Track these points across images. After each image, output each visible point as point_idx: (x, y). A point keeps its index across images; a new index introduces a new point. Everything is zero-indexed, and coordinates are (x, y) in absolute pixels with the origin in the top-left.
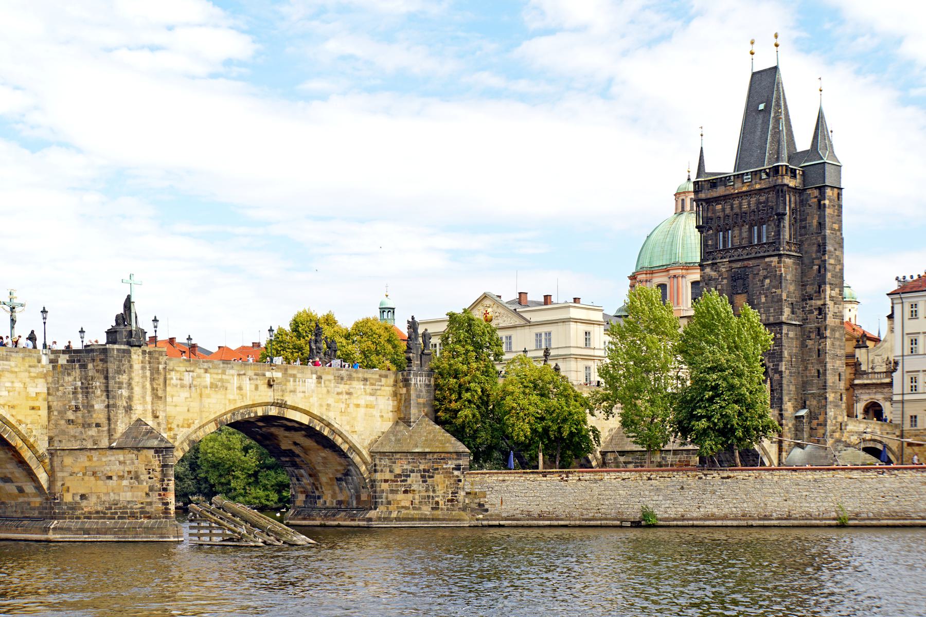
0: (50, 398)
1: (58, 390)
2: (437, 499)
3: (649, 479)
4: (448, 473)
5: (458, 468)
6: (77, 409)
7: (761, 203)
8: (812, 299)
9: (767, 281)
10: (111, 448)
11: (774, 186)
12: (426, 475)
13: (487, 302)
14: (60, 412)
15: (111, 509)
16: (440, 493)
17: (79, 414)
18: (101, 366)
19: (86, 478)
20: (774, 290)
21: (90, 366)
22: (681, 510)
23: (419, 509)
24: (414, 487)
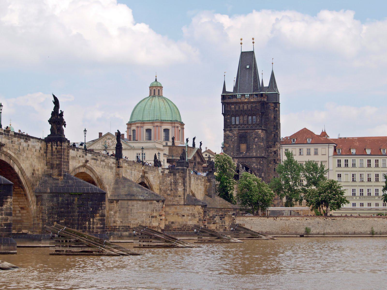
0: (161, 186)
1: (164, 182)
2: (226, 226)
3: (307, 220)
4: (230, 216)
5: (234, 214)
6: (171, 190)
7: (253, 107)
8: (271, 148)
9: (256, 139)
10: (185, 205)
11: (260, 101)
12: (222, 217)
13: (108, 137)
14: (164, 191)
15: (183, 227)
16: (227, 223)
17: (172, 192)
18: (181, 175)
19: (174, 216)
20: (259, 143)
21: (177, 174)
22: (318, 231)
23: (219, 230)
24: (217, 221)
